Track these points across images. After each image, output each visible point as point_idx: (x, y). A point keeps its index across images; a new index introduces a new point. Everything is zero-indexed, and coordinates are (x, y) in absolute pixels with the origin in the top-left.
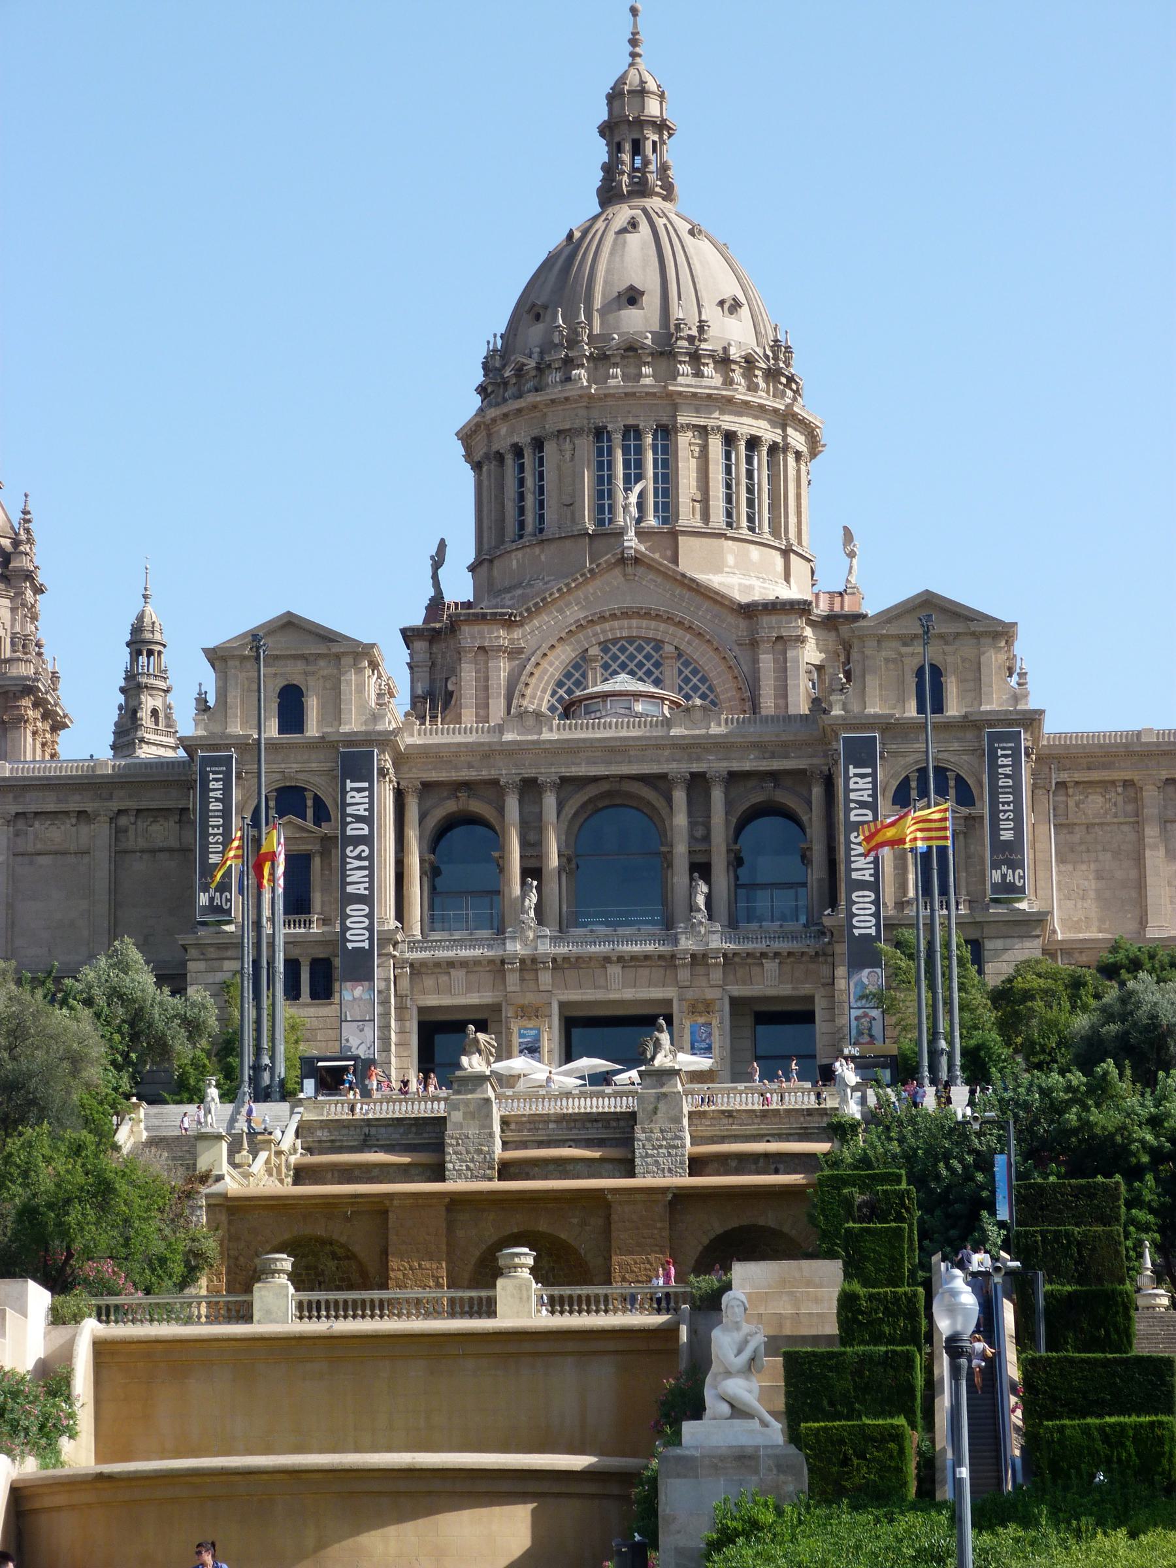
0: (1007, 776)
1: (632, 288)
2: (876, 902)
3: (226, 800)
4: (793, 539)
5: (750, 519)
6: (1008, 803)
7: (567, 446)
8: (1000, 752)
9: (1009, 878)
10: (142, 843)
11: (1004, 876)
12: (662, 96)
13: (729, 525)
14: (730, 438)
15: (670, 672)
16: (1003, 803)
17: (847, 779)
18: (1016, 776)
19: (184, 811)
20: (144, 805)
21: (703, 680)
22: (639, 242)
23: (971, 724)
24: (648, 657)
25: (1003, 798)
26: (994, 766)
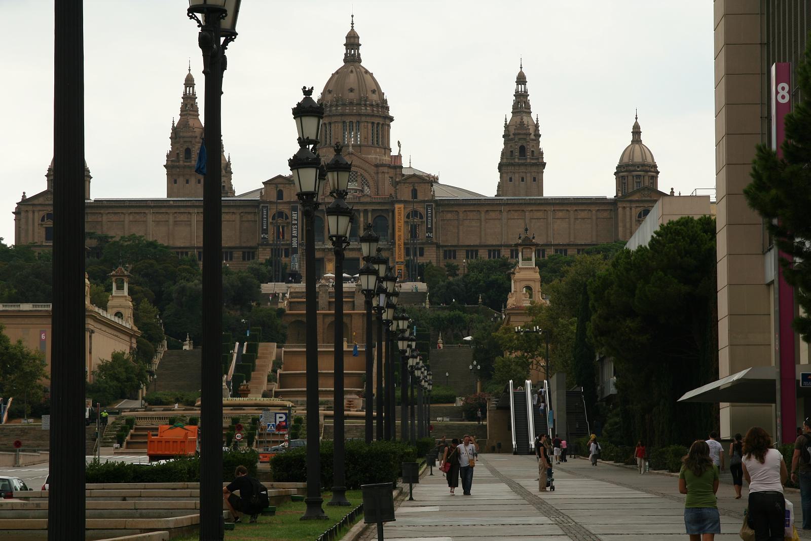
1: (351, 88)
3: (267, 215)
4: (387, 146)
5: (377, 141)
7: (337, 125)
10: (246, 220)
11: (429, 235)
12: (358, 38)
13: (372, 143)
14: (373, 123)
15: (359, 179)
18: (432, 214)
19: (256, 212)
20: (247, 211)
21: (366, 181)
22: (353, 77)
23: (424, 202)
24: (354, 175)
26: (427, 212)
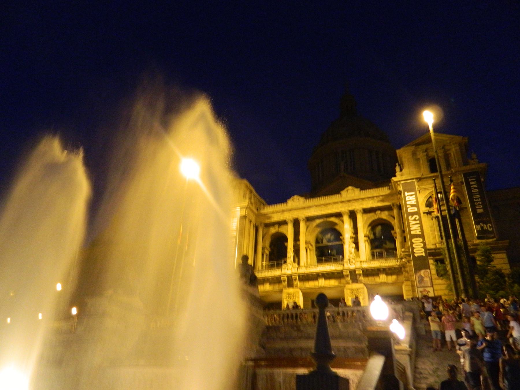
0: (475, 188)
2: (424, 242)
6: (478, 198)
8: (470, 180)
9: (485, 227)
11: (482, 227)
16: (476, 199)
17: (405, 197)
25: (475, 197)
